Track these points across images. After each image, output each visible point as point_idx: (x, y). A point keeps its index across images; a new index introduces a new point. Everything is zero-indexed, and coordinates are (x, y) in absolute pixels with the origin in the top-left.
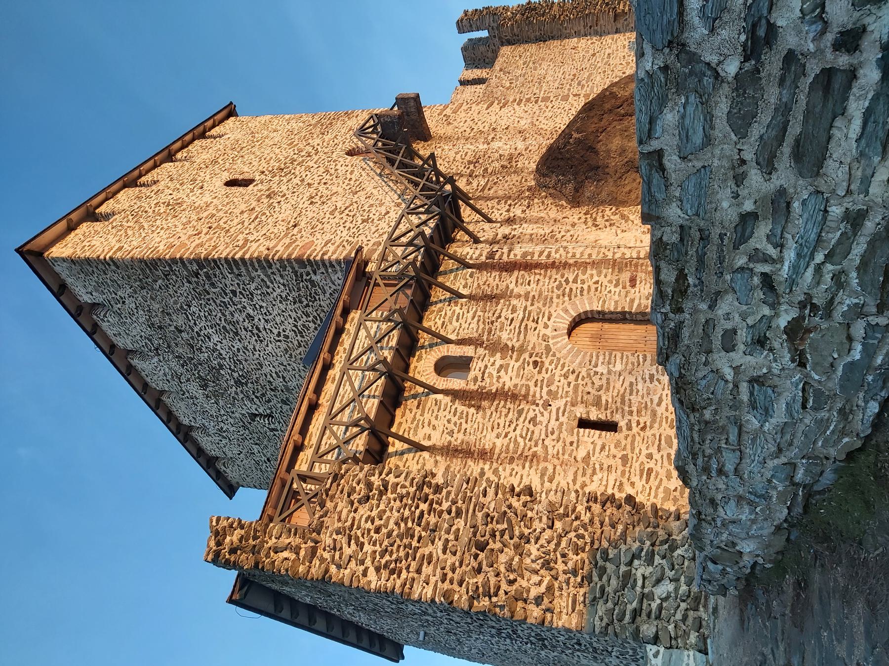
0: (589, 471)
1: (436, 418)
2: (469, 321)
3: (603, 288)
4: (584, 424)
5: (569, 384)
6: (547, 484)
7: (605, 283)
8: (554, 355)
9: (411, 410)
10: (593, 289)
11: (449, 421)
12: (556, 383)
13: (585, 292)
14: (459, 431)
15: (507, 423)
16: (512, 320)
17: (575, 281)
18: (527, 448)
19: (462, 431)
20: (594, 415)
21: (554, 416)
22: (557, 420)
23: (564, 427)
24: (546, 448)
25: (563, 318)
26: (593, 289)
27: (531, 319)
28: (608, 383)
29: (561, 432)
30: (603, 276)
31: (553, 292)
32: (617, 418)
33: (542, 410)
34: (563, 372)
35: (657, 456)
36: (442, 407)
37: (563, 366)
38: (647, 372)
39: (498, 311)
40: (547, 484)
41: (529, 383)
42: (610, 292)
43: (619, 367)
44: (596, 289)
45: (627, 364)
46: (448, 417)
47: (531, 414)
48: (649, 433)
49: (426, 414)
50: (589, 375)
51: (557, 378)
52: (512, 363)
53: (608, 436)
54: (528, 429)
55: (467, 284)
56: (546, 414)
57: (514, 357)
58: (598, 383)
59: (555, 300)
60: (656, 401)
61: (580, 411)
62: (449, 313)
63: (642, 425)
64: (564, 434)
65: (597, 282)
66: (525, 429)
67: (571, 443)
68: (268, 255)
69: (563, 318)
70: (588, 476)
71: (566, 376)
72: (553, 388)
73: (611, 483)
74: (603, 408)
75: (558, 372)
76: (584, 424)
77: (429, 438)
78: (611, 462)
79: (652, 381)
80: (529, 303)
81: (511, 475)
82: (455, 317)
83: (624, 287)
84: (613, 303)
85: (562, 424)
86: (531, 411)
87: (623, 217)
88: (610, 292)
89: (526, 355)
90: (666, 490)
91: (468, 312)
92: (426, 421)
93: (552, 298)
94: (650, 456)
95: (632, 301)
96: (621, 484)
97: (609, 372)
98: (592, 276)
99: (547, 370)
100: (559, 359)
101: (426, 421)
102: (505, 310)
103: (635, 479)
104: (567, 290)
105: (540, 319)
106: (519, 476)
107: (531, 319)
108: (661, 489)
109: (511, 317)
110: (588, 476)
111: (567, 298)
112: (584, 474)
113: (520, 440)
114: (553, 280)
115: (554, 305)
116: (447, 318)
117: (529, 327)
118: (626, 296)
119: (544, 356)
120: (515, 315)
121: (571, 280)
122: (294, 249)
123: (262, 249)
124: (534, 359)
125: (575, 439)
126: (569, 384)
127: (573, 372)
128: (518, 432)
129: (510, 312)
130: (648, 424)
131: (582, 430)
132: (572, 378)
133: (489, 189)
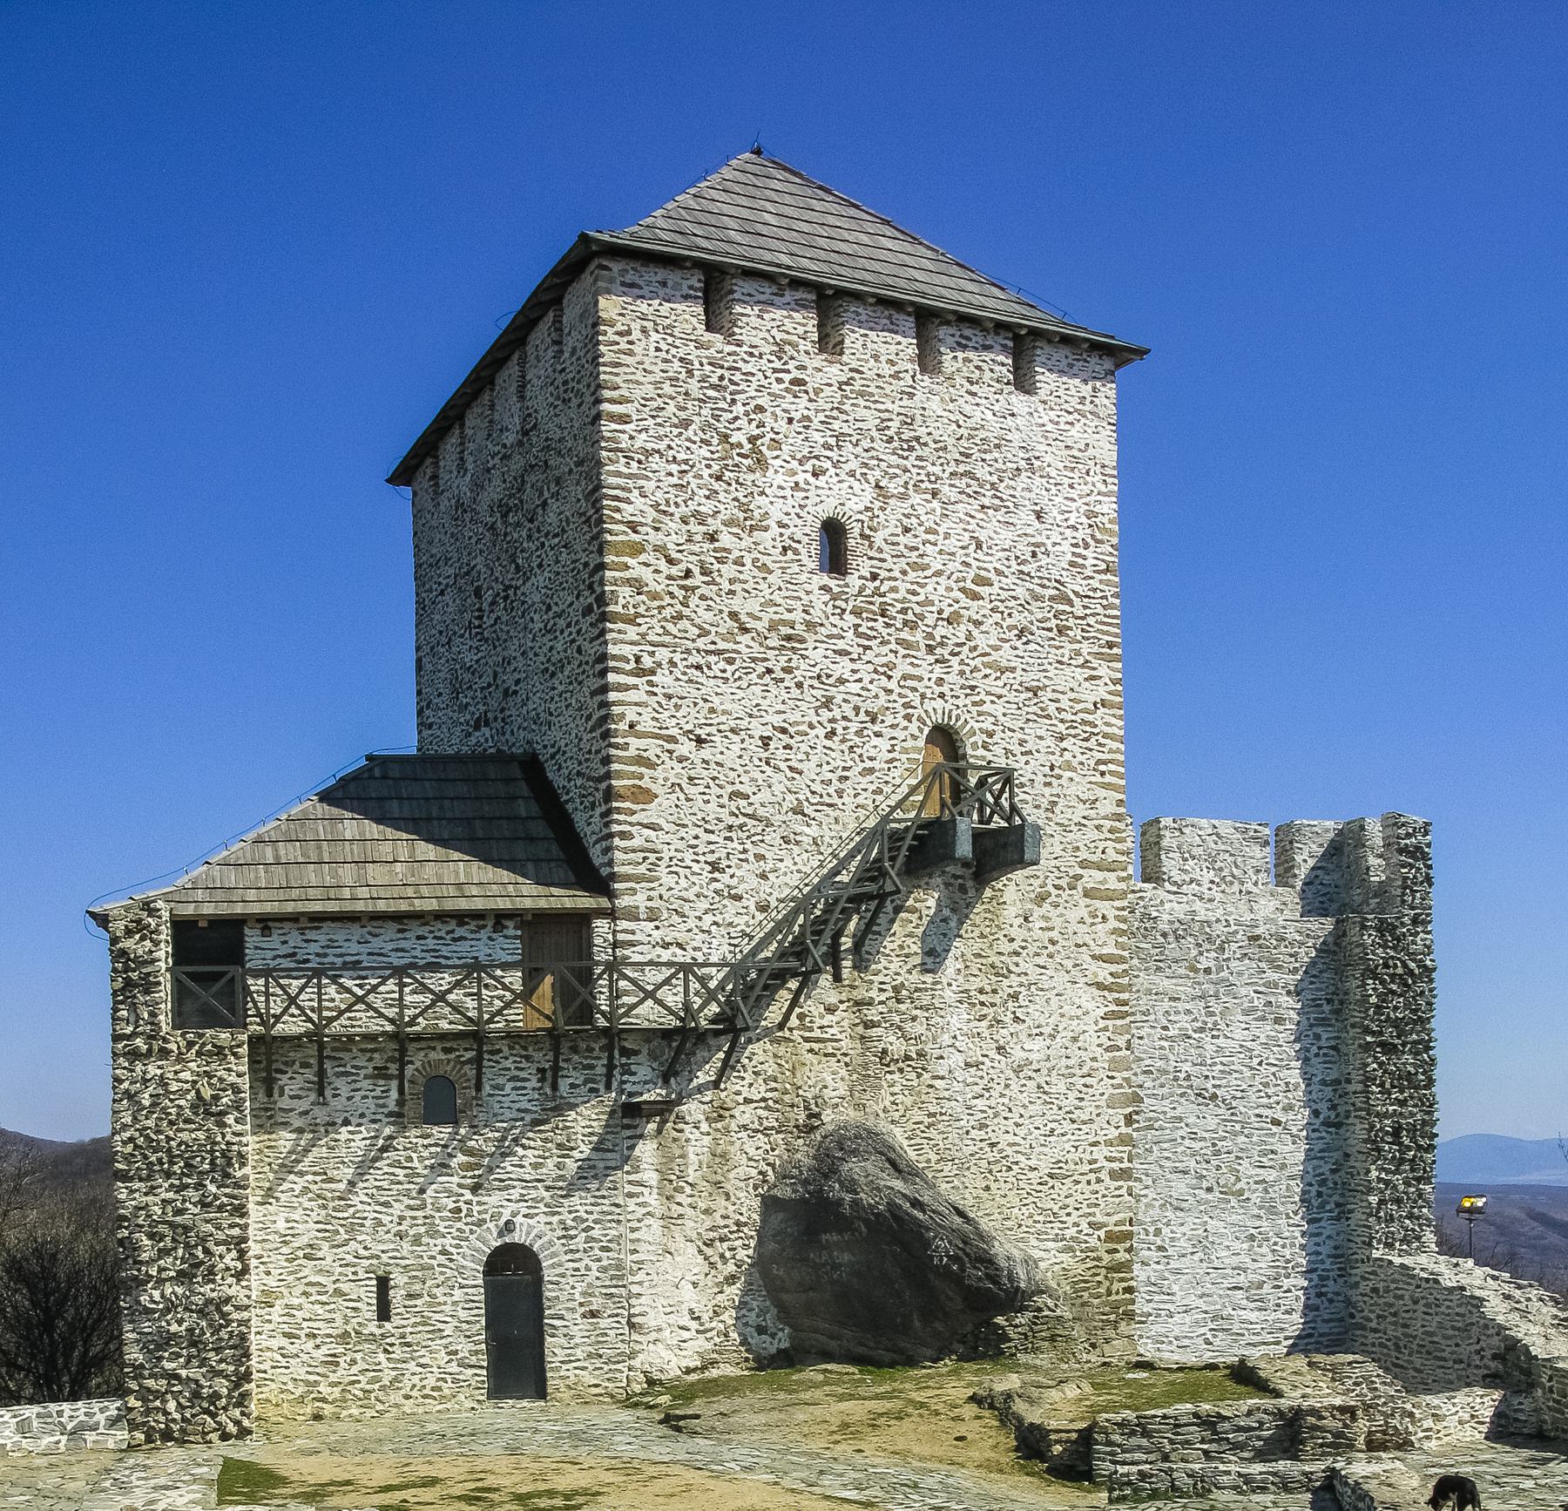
0: (324, 1298)
1: (366, 1097)
2: (517, 1106)
3: (579, 1278)
4: (383, 1284)
5: (433, 1257)
6: (300, 1253)
7: (587, 1279)
8: (472, 1232)
9: (370, 1059)
10: (576, 1265)
11: (362, 1115)
12: (432, 1242)
13: (569, 1257)
14: (349, 1132)
15: (369, 1191)
16: (522, 1166)
17: (590, 1239)
18: (342, 1222)
19: (351, 1137)
20: (397, 1296)
21: (384, 1247)
22: (383, 1252)
23: (375, 1262)
24: (345, 1243)
25: (528, 1233)
26: (576, 1265)
27: (524, 1192)
28: (439, 1304)
29: (368, 1258)
30: (598, 1274)
31: (570, 1212)
32: (396, 1321)
33: (393, 1231)
34: (448, 1247)
35: (354, 1370)
36: (381, 1101)
37: (458, 1246)
38: (459, 1348)
39: (532, 1144)
40: (300, 1253)
41: (430, 1207)
42: (573, 1287)
43: (463, 1315)
44: (577, 1270)
45: (467, 1322)
46: (367, 1112)
47: (385, 1219)
48: (382, 1357)
49: (368, 1081)
50: (448, 1279)
51: (439, 1241)
52: (455, 1179)
53: (369, 1311)
54: (365, 1218)
55: (579, 1086)
56: (390, 1236)
57: (462, 1181)
58: (438, 1292)
59: (555, 1219)
60: (422, 1361)
61: (398, 1279)
62: (523, 1074)
63: (390, 1349)
64: (366, 1263)
65: (588, 1268)
66: (366, 1215)
67: (355, 1273)
68: (615, 733)
69: (528, 1233)
70: (319, 1298)
71: (444, 1252)
72: (425, 1240)
73: (315, 1325)
74: (407, 1303)
75: (448, 1241)
76: (383, 1284)
77: (335, 1096)
78: (339, 1322)
79: (449, 1353)
80: (548, 1183)
81: (304, 1209)
82: (519, 1084)
83: (581, 1304)
84: (554, 1294)
85: (378, 1257)
86: (390, 1218)
87: (731, 1279)
88: (573, 1287)
89: (468, 1195)
90: (316, 1383)
91: (530, 1101)
92: (358, 1085)
93: (559, 1213)
94: (354, 1362)
95: (562, 1318)
96: (315, 1336)
97: (455, 1303)
98: (599, 1260)
99: (450, 1227)
100: (467, 1239)
101: (358, 1085)
102: (536, 1153)
103: (324, 1350)
104: (572, 1232)
105: (525, 1204)
106: (306, 1218)
107: (524, 1192)
108: (319, 1378)
109: (526, 1164)
110: (319, 1298)
111: (561, 1233)
112: (319, 1293)
113: (351, 1210)
114: (589, 1208)
115: (549, 1219)
116: (517, 1073)
117: (511, 1191)
118: (568, 1309)
119: (469, 1220)
120: (529, 1169)
121: (592, 1233)
122: (633, 776)
123: (631, 714)
124: (464, 1207)
125: (362, 1275)
126: (433, 1257)
127: (451, 1260)
128: (360, 1207)
129: (534, 1160)
130: (392, 1356)
131: (374, 1282)
132: (441, 1259)
133: (811, 1051)
